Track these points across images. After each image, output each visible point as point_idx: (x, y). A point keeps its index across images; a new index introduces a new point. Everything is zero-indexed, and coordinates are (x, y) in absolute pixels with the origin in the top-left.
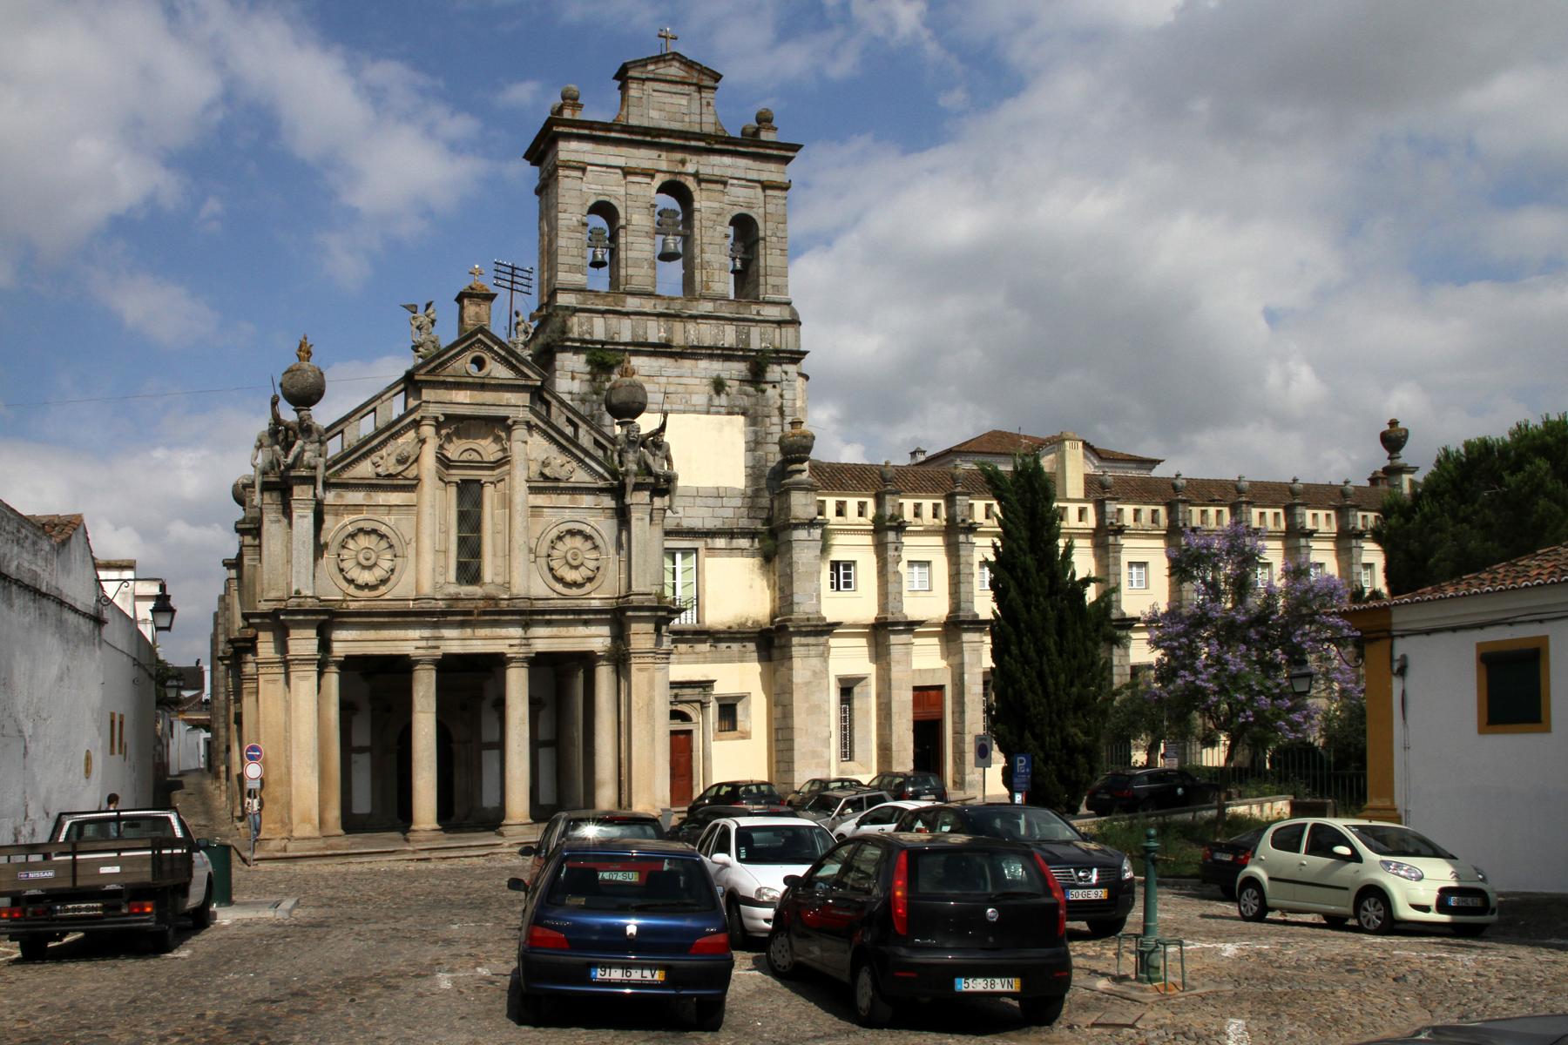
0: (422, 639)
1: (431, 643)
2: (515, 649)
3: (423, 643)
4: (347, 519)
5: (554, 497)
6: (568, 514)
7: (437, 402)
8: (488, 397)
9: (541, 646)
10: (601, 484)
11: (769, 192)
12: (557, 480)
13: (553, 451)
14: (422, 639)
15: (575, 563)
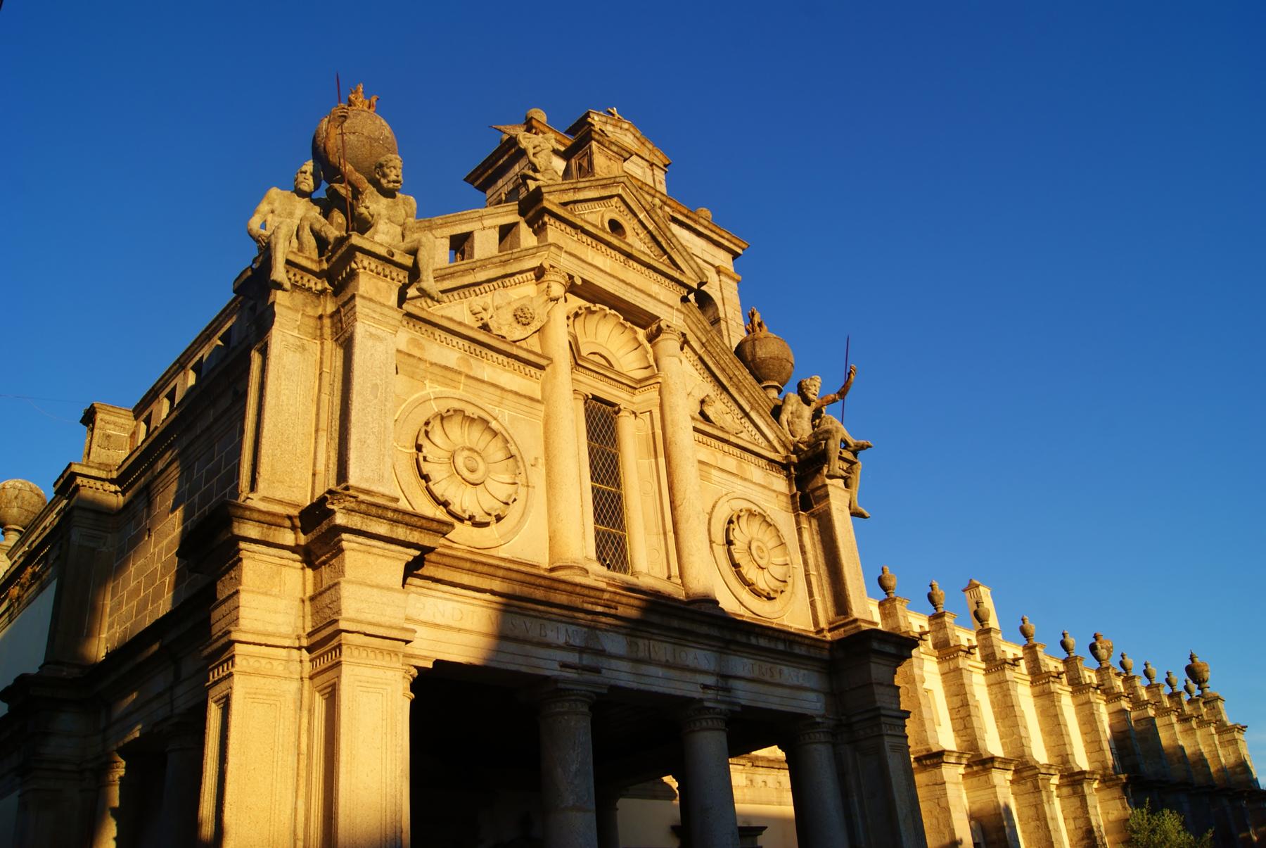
0: (568, 647)
1: (587, 660)
2: (710, 694)
3: (573, 658)
4: (432, 389)
5: (719, 455)
6: (739, 487)
7: (571, 254)
8: (634, 274)
9: (744, 694)
10: (772, 455)
11: (723, 278)
12: (722, 429)
13: (709, 389)
14: (568, 647)
15: (762, 563)
